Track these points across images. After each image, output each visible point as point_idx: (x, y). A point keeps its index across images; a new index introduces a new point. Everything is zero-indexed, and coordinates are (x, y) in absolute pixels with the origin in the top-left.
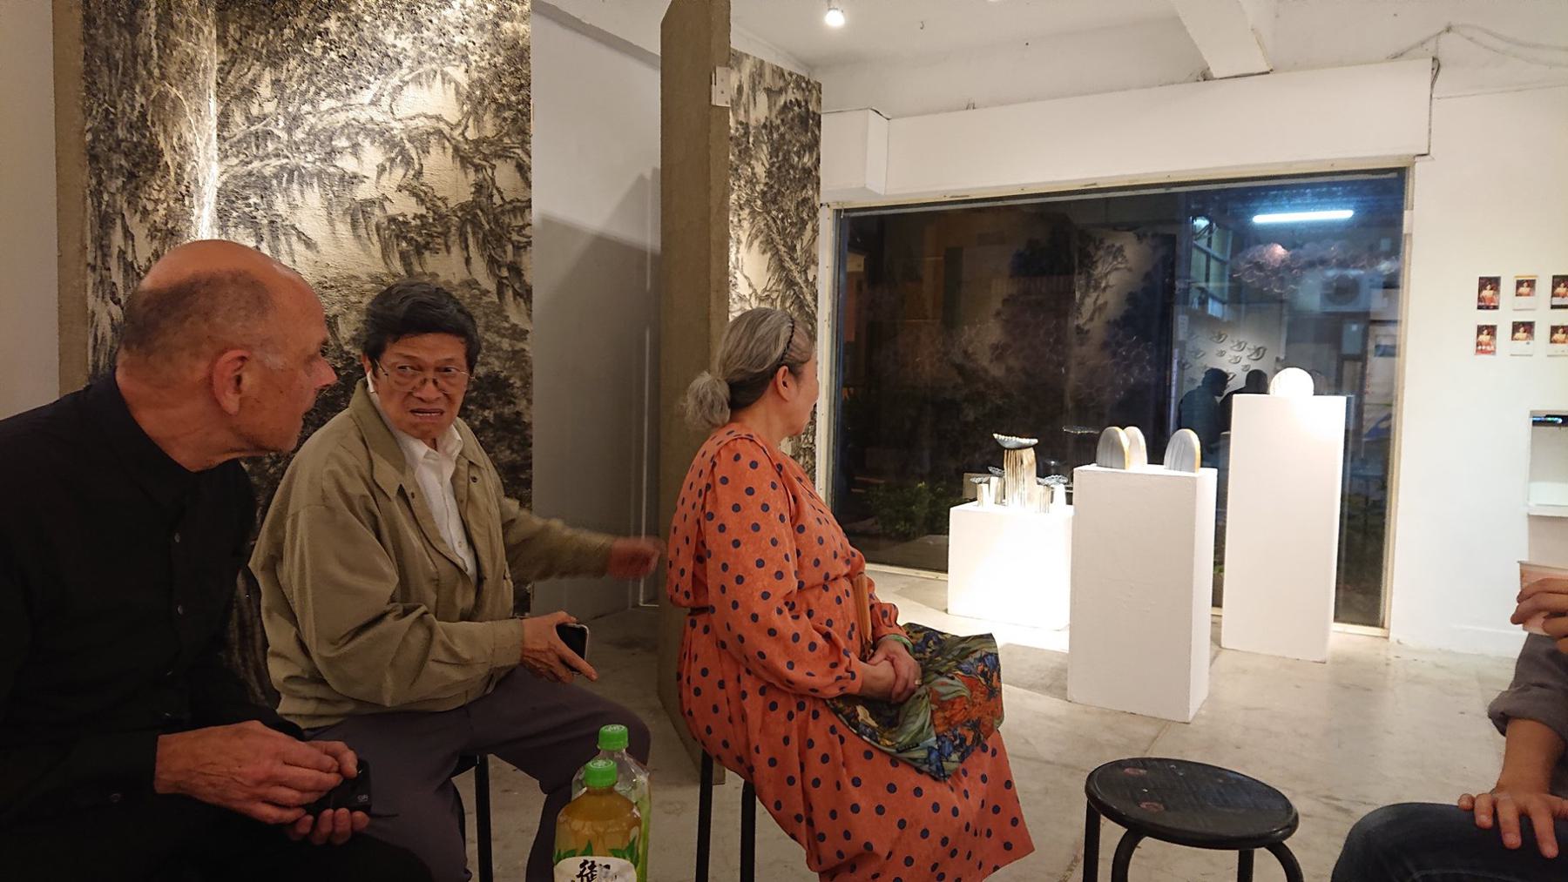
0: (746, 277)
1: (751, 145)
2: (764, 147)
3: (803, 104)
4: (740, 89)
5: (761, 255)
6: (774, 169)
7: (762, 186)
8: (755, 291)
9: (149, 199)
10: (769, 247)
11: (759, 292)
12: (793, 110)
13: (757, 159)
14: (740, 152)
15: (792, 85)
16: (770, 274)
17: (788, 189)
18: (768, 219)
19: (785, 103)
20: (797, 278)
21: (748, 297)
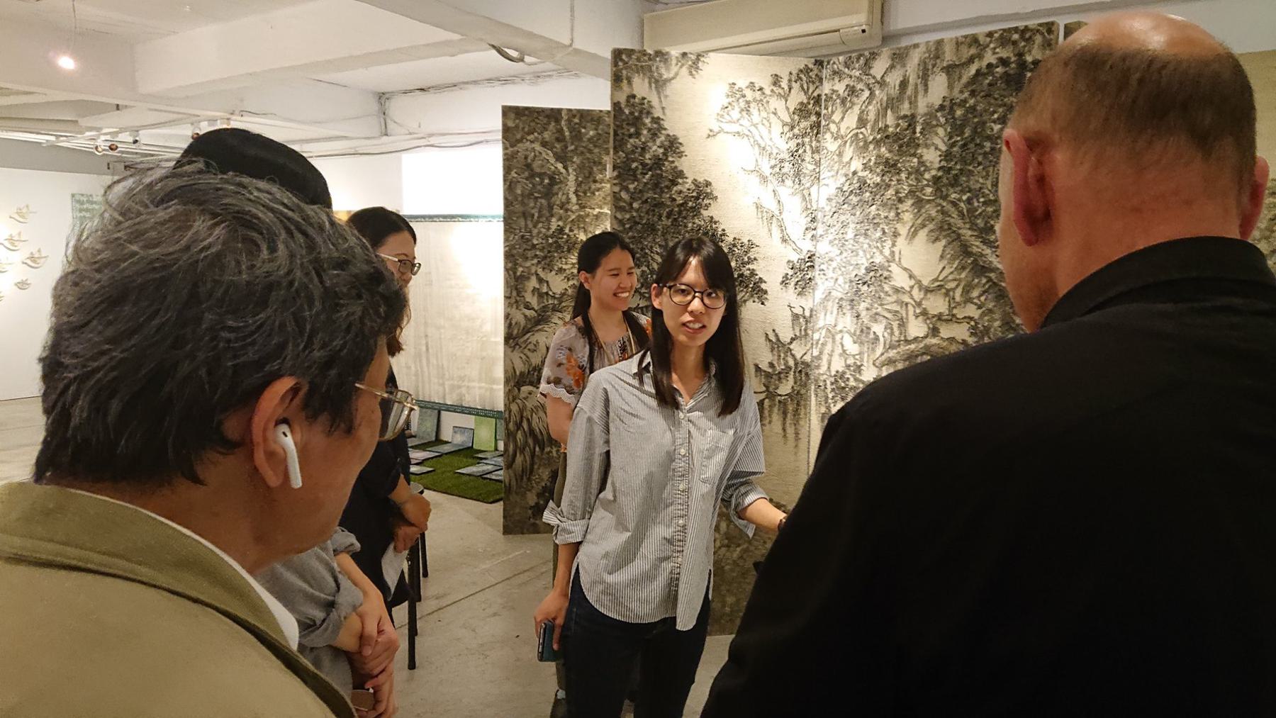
0: (905, 269)
1: (918, 135)
2: (941, 131)
3: (1013, 59)
4: (904, 84)
5: (931, 244)
6: (955, 149)
7: (934, 172)
8: (919, 282)
9: (566, 264)
10: (944, 233)
11: (925, 283)
12: (993, 75)
13: (927, 146)
14: (901, 146)
15: (992, 46)
16: (945, 262)
17: (980, 164)
18: (944, 204)
19: (978, 71)
20: (995, 263)
21: (908, 289)
